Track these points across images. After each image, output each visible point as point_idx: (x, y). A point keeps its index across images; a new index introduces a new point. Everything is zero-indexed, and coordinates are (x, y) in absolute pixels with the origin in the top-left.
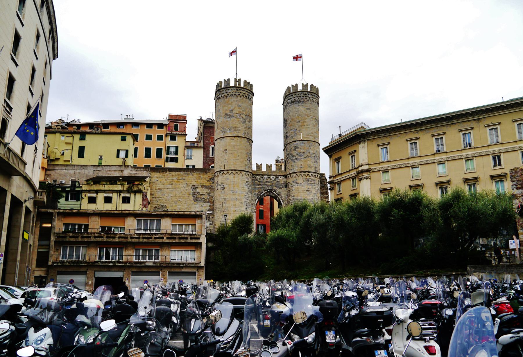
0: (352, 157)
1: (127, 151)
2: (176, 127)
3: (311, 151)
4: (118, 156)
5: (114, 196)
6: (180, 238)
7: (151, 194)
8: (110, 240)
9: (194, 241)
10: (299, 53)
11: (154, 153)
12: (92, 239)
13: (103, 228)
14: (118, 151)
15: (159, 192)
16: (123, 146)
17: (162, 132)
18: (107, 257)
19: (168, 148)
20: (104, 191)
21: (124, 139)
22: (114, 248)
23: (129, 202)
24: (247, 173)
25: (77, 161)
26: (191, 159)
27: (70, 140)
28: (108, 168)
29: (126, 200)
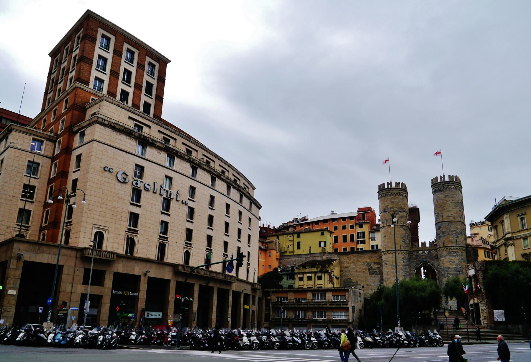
0: (502, 225)
1: (325, 242)
2: (364, 216)
3: (452, 229)
4: (320, 246)
5: (313, 275)
6: (337, 304)
7: (341, 271)
8: (299, 306)
9: (344, 306)
10: (438, 151)
11: (348, 238)
12: (290, 306)
13: (296, 299)
14: (320, 243)
15: (346, 269)
16: (322, 239)
17: (353, 223)
18: (299, 316)
19: (358, 233)
20: (307, 273)
21: (322, 234)
22: (302, 311)
23: (321, 279)
24: (402, 252)
25: (297, 252)
26: (375, 240)
27: (291, 238)
28: (314, 255)
29: (320, 278)
